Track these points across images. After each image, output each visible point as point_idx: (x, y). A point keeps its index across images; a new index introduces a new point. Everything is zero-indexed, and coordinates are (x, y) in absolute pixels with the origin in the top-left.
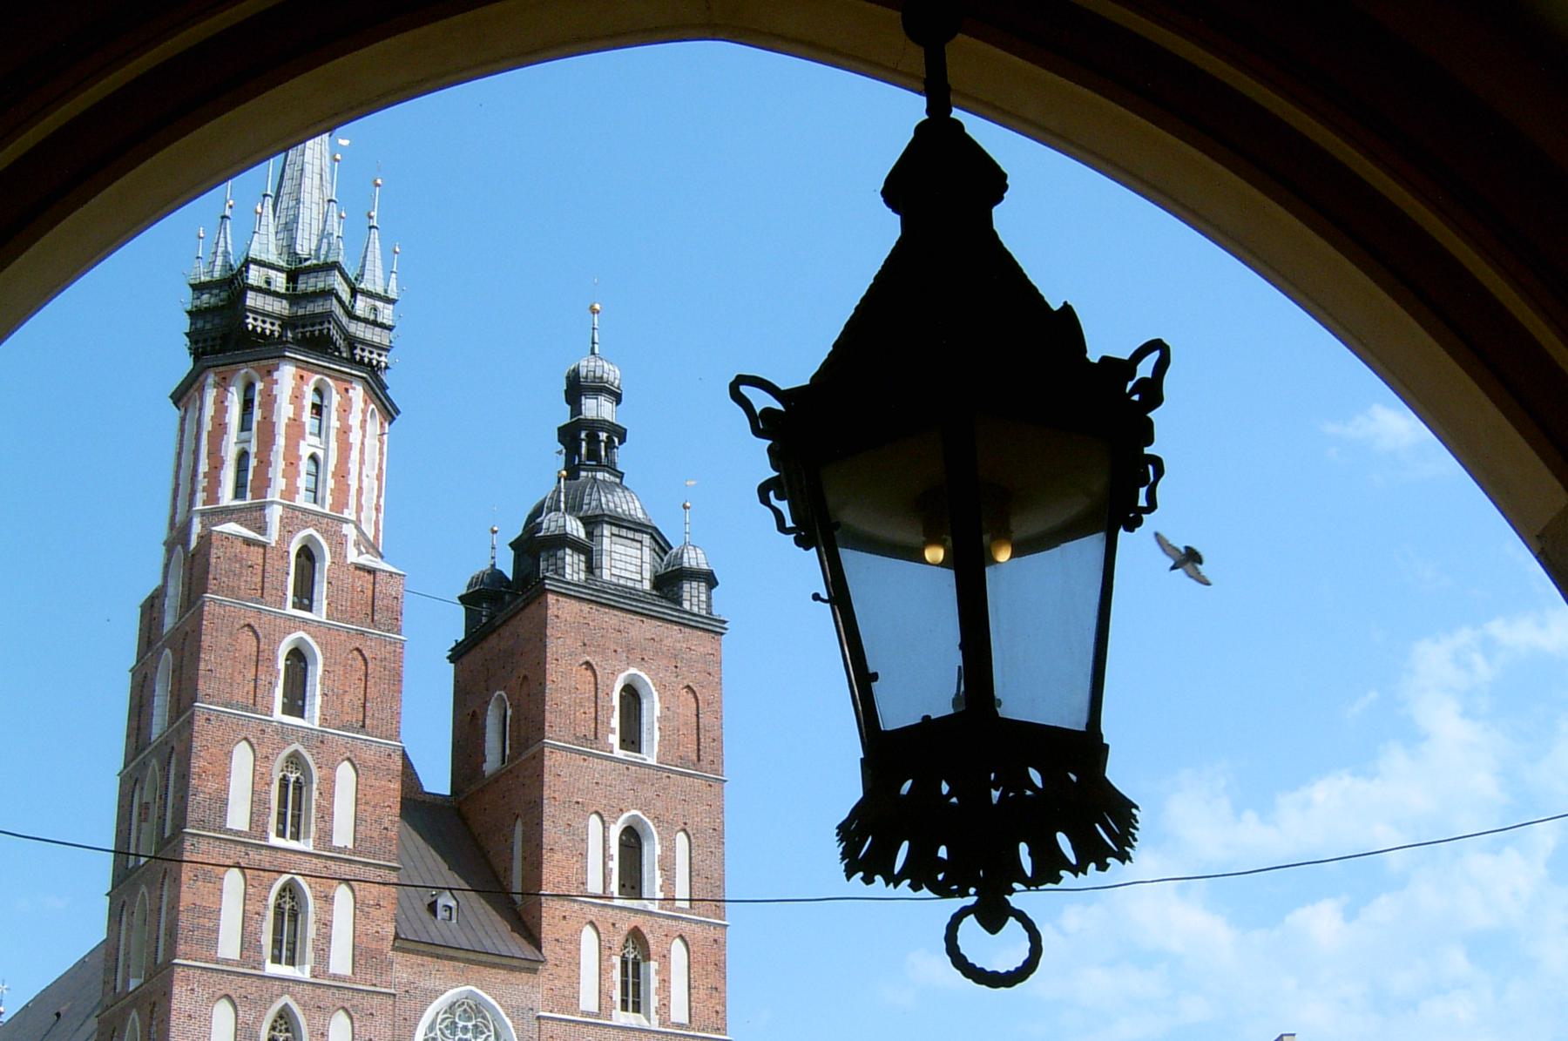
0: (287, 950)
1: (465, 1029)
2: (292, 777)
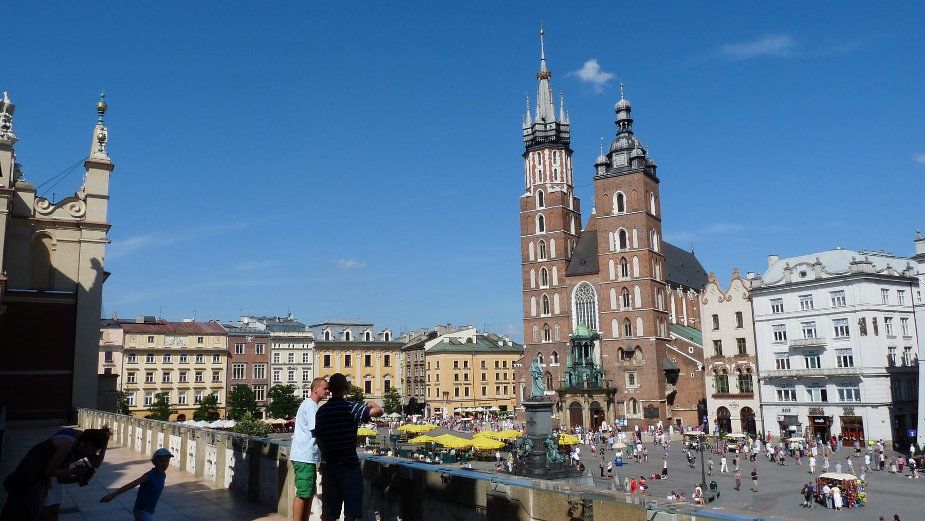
1: (585, 290)
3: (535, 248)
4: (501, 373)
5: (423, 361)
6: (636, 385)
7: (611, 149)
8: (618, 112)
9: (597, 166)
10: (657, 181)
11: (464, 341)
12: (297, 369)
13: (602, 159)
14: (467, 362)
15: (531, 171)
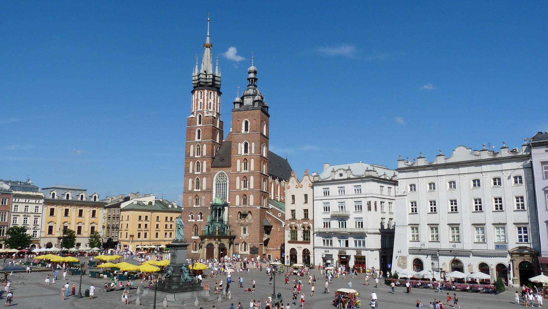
1: (221, 177)
2: (199, 148)
3: (194, 149)
4: (169, 224)
5: (118, 215)
6: (247, 234)
7: (243, 94)
8: (250, 73)
9: (235, 103)
10: (268, 116)
11: (147, 203)
12: (30, 216)
13: (238, 99)
14: (147, 216)
15: (196, 102)
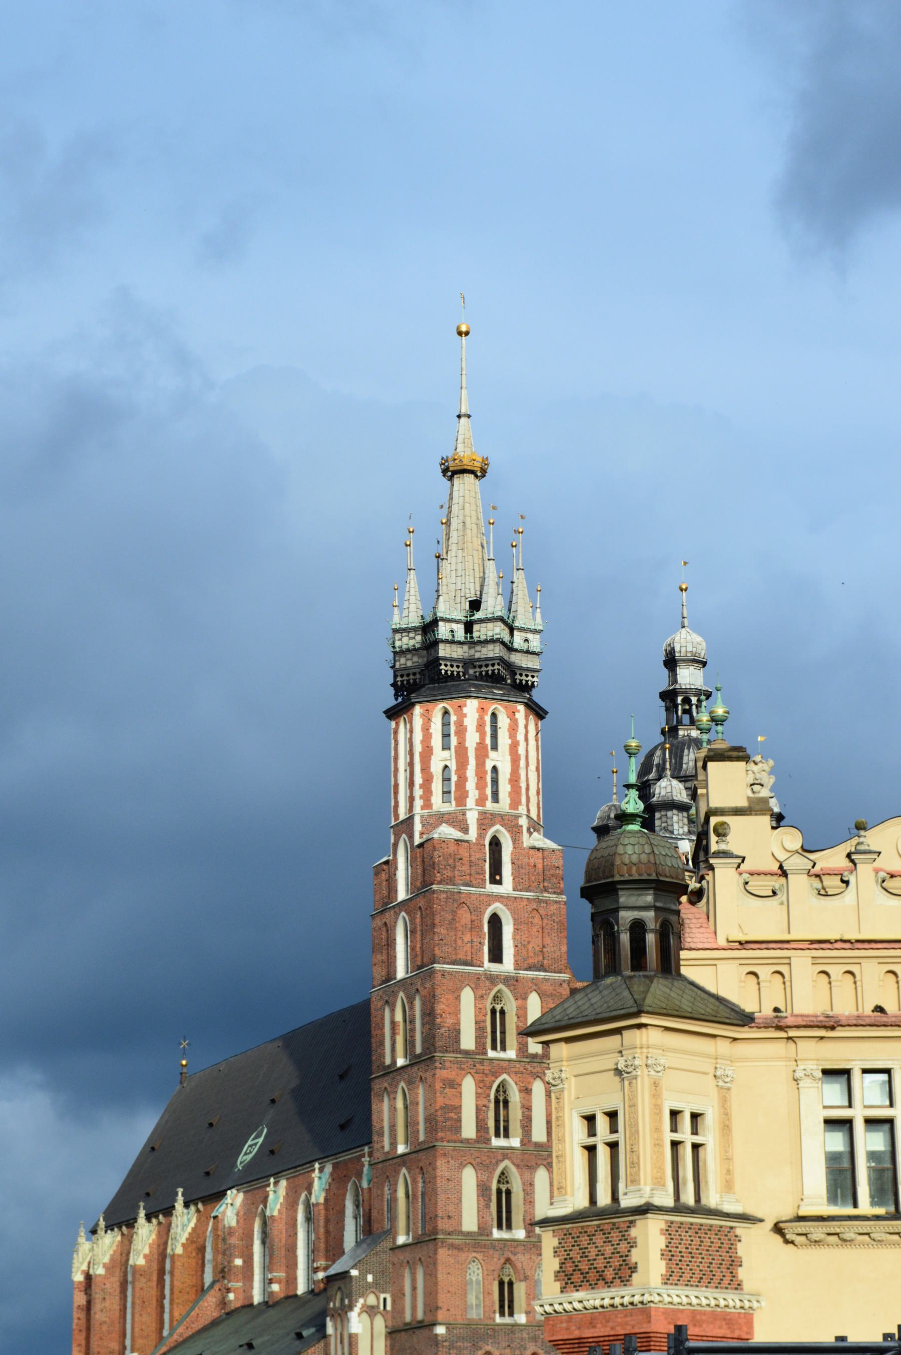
0: (503, 1130)
2: (498, 1008)
3: (479, 1010)
